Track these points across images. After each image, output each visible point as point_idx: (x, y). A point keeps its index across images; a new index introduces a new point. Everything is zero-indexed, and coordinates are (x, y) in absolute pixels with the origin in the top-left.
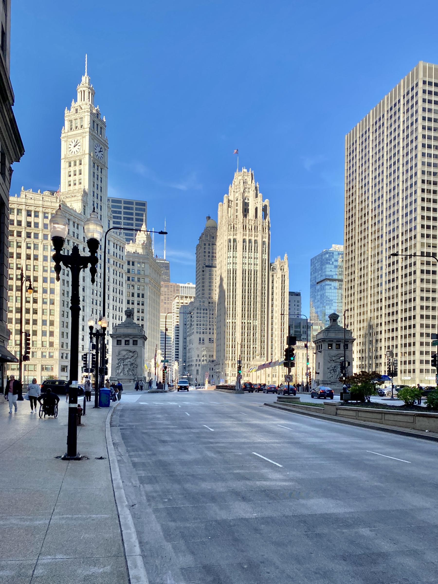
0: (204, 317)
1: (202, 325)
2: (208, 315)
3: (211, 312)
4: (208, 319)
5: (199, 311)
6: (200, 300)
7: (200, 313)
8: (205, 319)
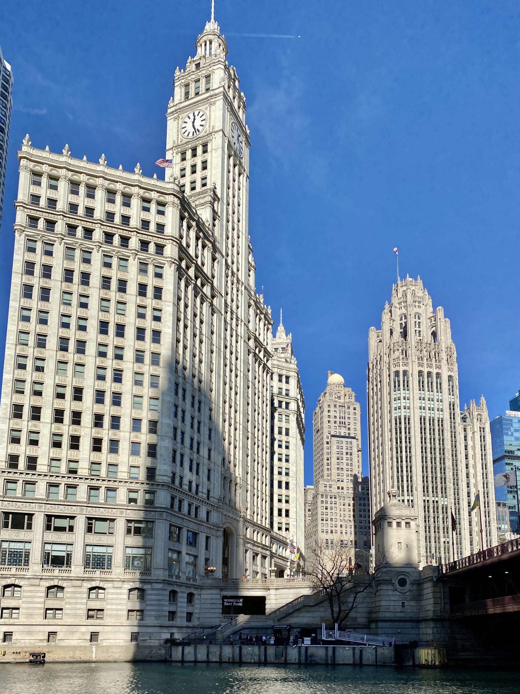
0: (331, 508)
1: (329, 520)
2: (337, 506)
3: (342, 501)
4: (338, 511)
5: (324, 499)
6: (326, 483)
7: (327, 502)
8: (333, 511)
